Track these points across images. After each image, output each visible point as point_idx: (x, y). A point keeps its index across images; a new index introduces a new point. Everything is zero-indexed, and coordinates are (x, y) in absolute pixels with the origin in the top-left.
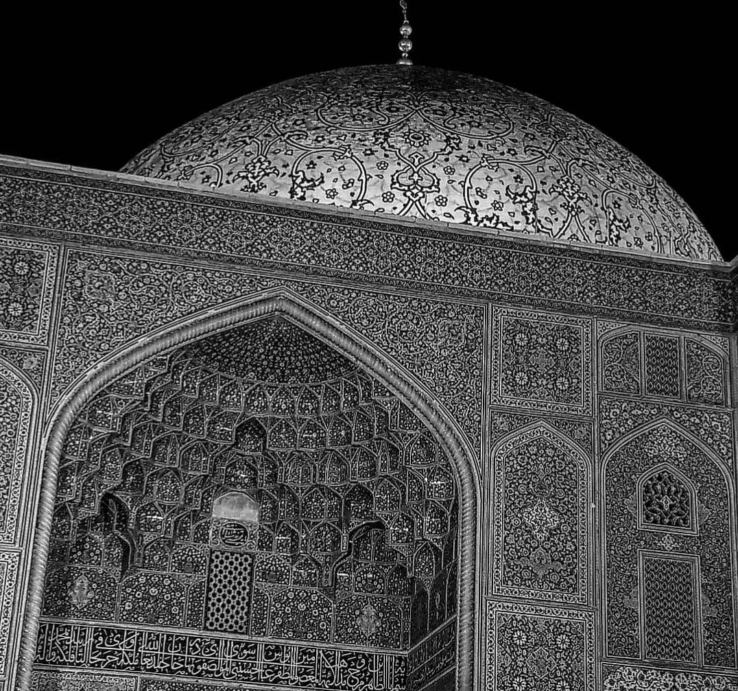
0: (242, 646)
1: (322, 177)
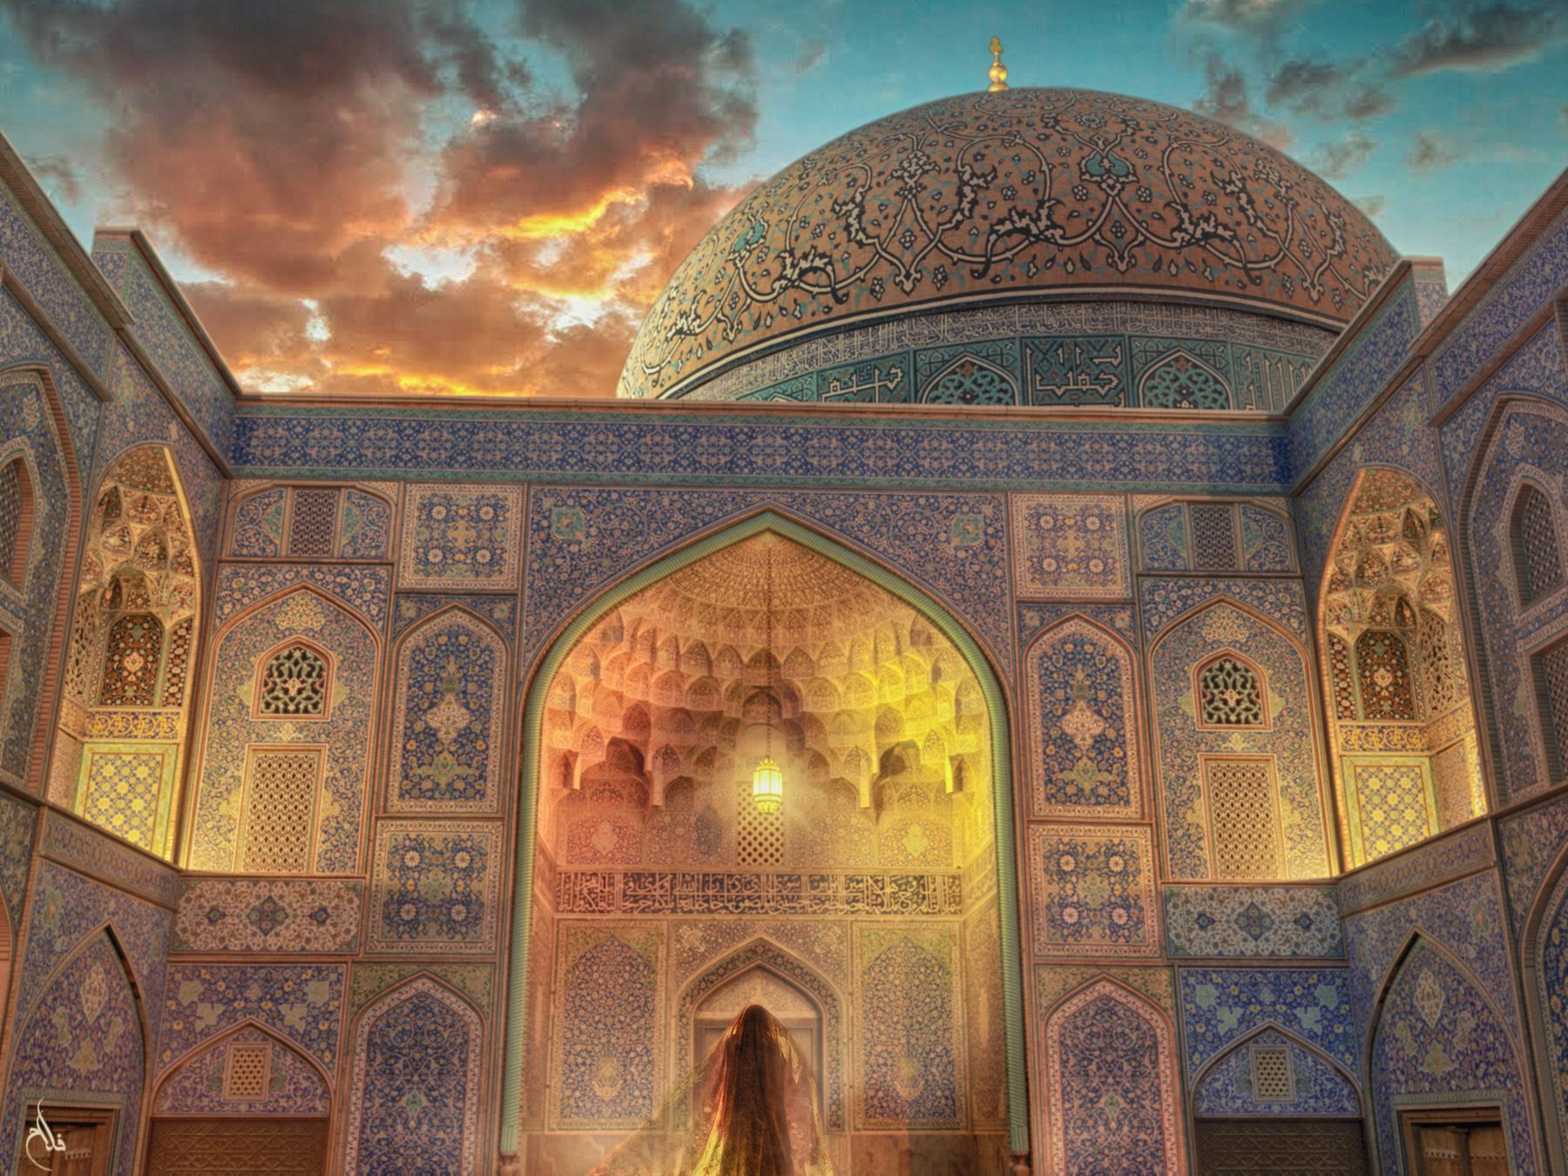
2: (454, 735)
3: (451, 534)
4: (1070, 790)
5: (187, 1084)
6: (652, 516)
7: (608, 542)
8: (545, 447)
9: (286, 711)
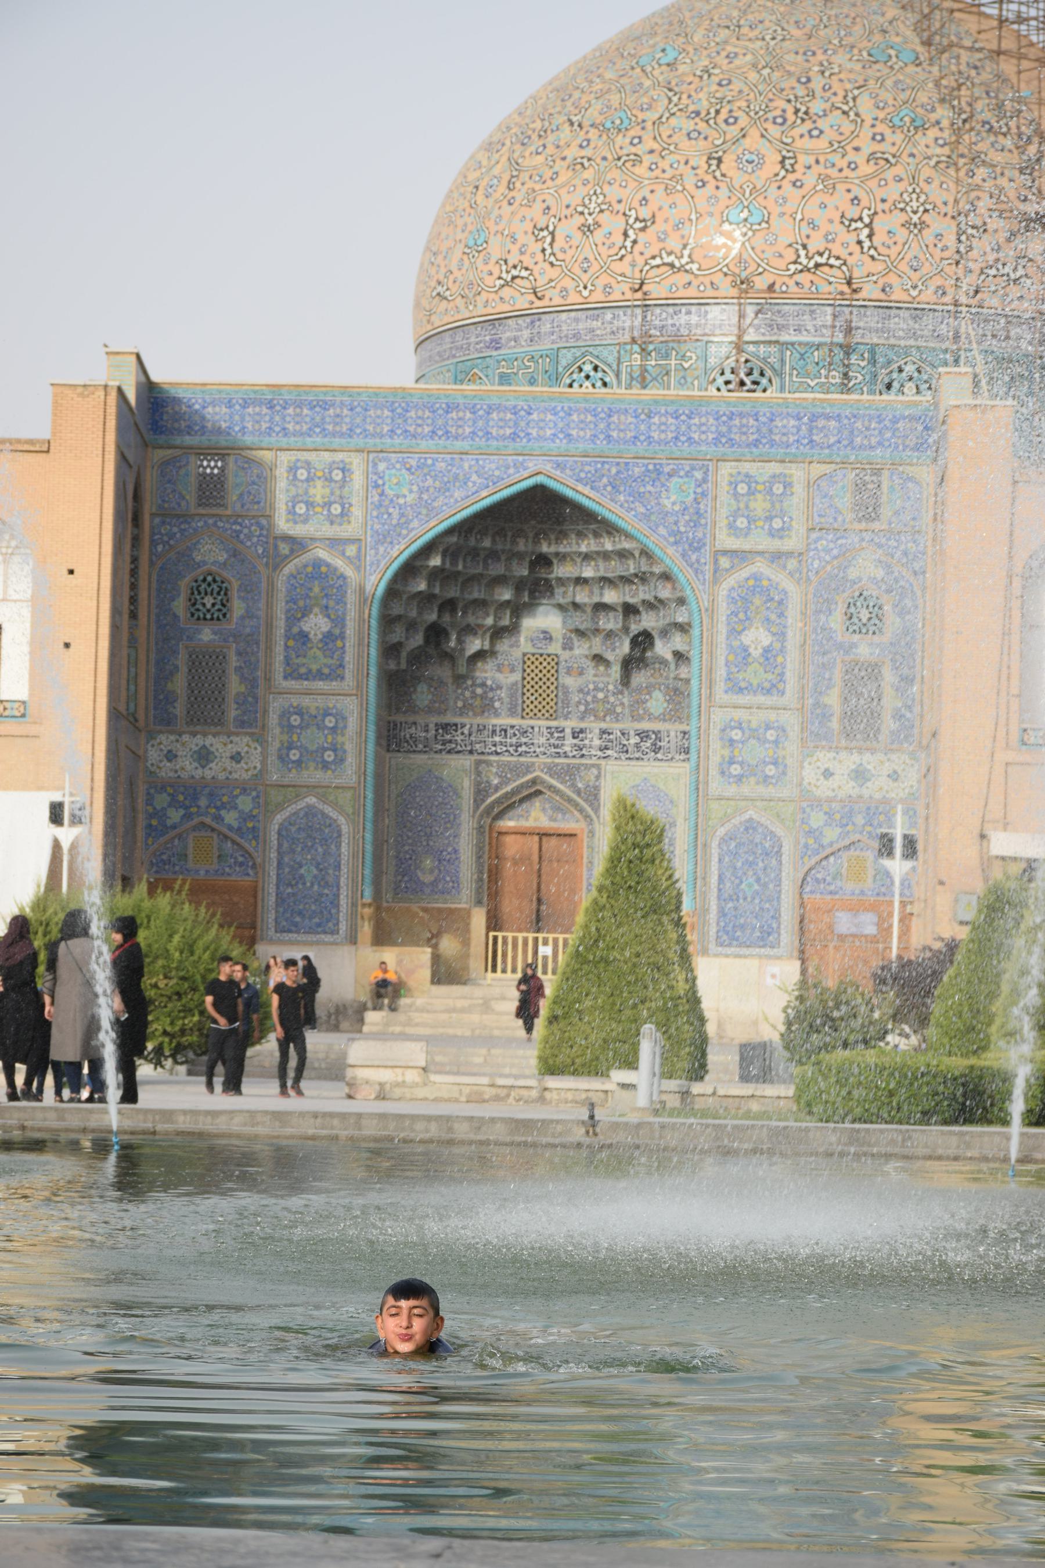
1: (654, 216)
2: (320, 636)
3: (312, 491)
4: (743, 685)
5: (164, 857)
6: (456, 477)
7: (425, 497)
8: (379, 421)
9: (205, 619)
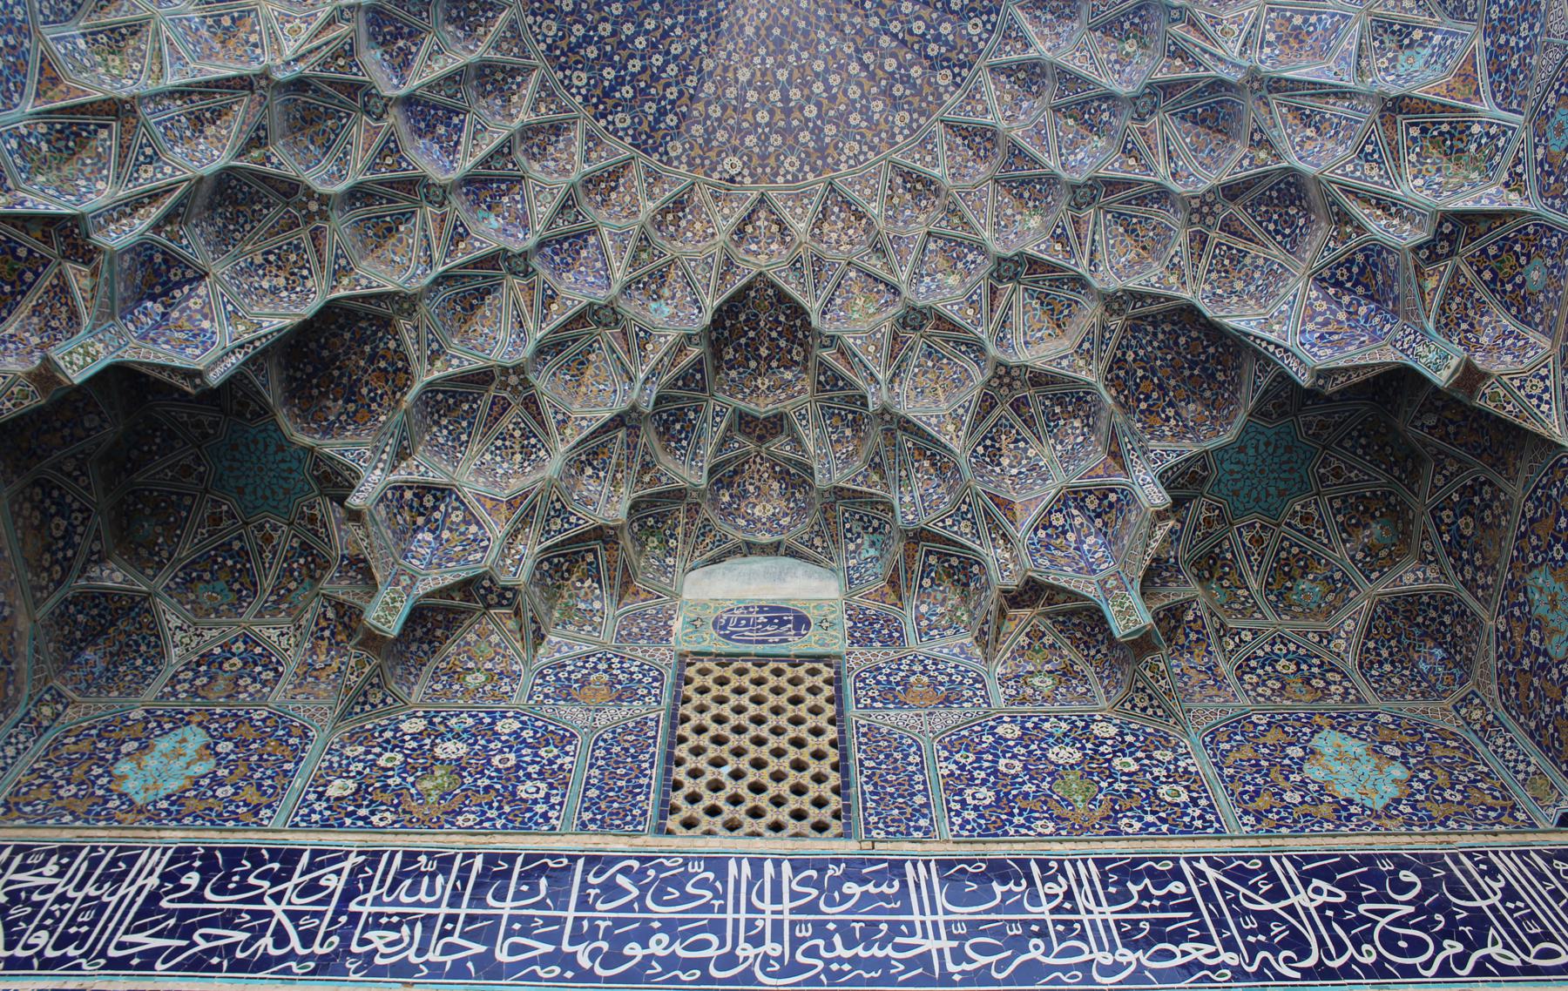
0: (833, 871)
